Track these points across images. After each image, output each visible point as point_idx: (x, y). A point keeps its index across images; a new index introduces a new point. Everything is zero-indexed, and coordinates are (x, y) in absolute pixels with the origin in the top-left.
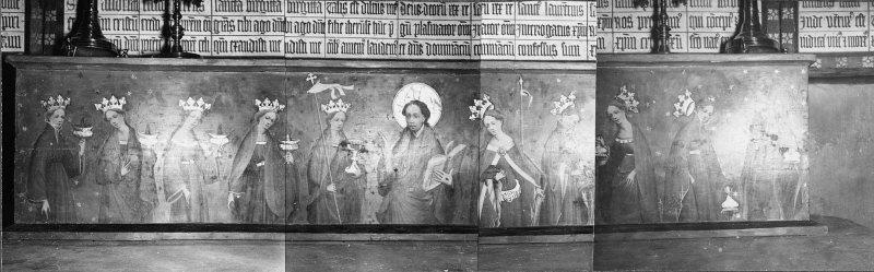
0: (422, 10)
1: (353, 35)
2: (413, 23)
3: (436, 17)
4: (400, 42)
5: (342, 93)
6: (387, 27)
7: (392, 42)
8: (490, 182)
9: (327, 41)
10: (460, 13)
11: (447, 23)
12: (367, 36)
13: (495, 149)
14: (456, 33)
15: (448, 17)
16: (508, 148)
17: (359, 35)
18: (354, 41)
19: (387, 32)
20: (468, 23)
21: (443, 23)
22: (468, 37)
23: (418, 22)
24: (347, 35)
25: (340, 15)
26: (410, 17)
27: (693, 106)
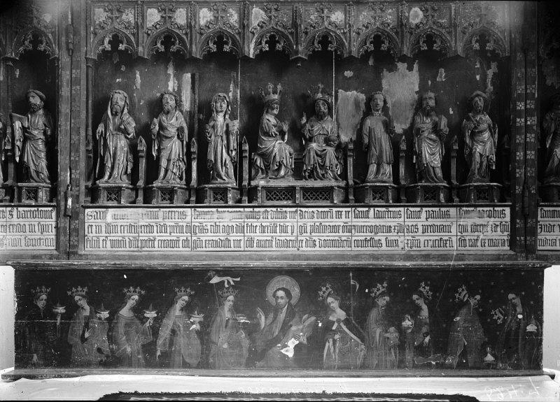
0: (315, 215)
1: (265, 234)
2: (309, 224)
3: (326, 220)
4: (299, 238)
5: (232, 283)
6: (289, 228)
7: (293, 238)
8: (331, 340)
9: (246, 239)
10: (343, 216)
12: (275, 234)
13: (335, 319)
14: (341, 231)
15: (335, 220)
16: (343, 318)
17: (269, 234)
18: (265, 238)
20: (350, 224)
21: (331, 224)
25: (255, 220)
27: (467, 296)
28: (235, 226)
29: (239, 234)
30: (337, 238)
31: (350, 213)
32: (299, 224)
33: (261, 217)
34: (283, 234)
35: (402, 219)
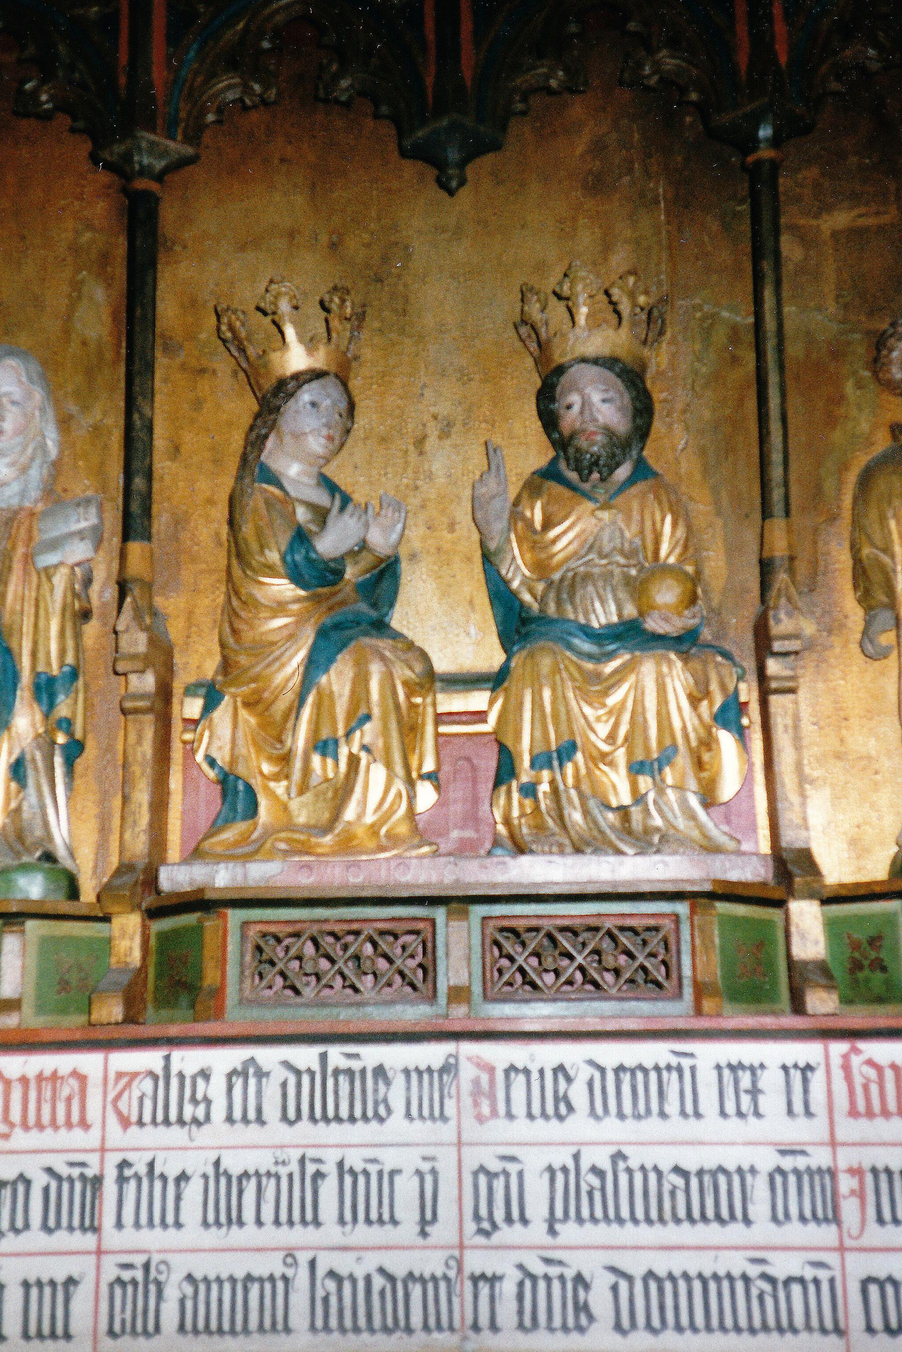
0: (578, 1094)
1: (237, 1236)
2: (534, 1163)
3: (652, 1127)
4: (475, 1262)
6: (406, 1190)
7: (432, 1263)
9: (110, 1272)
10: (772, 1103)
11: (709, 1158)
14: (760, 1208)
15: (712, 1125)
17: (271, 1235)
18: (239, 1266)
20: (820, 1158)
21: (691, 1160)
22: (827, 1234)
23: (562, 1157)
25: (176, 1135)
26: (522, 1128)
28: (40, 1180)
29: (62, 1239)
30: (737, 1264)
31: (817, 1081)
32: (473, 1158)
33: (219, 1111)
34: (363, 1234)
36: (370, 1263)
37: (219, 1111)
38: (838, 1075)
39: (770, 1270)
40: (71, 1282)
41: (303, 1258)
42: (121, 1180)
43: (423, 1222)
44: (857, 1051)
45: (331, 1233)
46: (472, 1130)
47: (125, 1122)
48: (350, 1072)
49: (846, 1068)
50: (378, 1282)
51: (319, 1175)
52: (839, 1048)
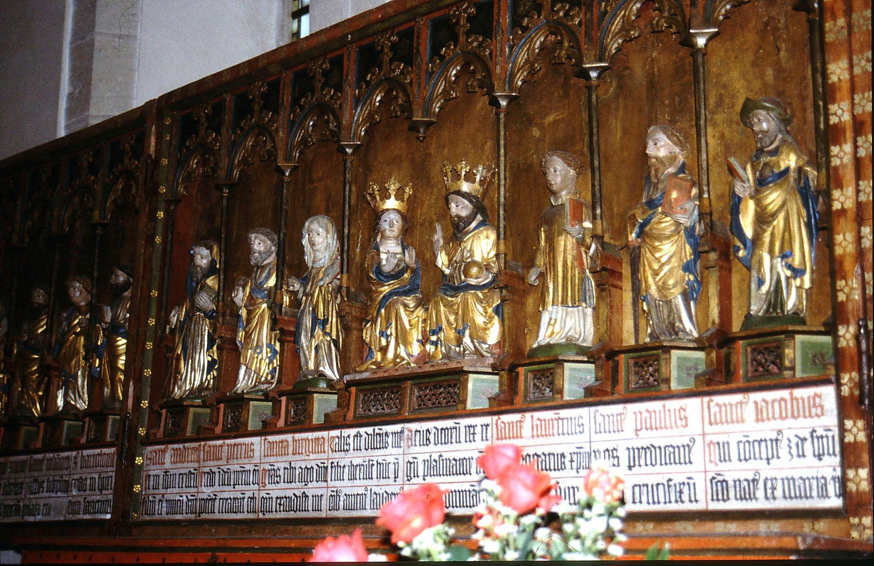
0: (432, 437)
2: (421, 458)
3: (449, 447)
7: (396, 490)
9: (330, 493)
10: (478, 437)
19: (392, 475)
23: (427, 457)
24: (350, 483)
25: (343, 454)
26: (418, 449)
30: (466, 487)
31: (489, 428)
33: (352, 448)
35: (585, 437)
36: (384, 489)
37: (352, 448)
38: (494, 426)
39: (475, 488)
40: (322, 495)
41: (369, 488)
42: (332, 467)
43: (395, 478)
44: (712, 401)
45: (375, 481)
46: (595, 437)
47: (332, 451)
48: (379, 434)
49: (497, 424)
50: (385, 495)
51: (373, 465)
52: (495, 418)
